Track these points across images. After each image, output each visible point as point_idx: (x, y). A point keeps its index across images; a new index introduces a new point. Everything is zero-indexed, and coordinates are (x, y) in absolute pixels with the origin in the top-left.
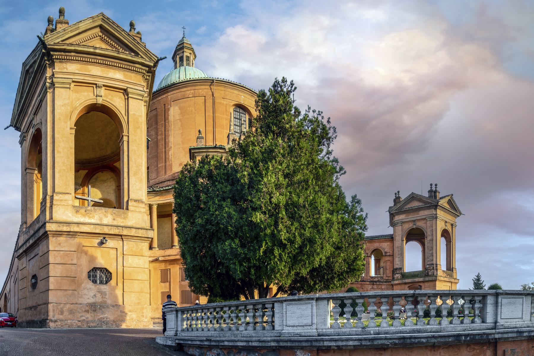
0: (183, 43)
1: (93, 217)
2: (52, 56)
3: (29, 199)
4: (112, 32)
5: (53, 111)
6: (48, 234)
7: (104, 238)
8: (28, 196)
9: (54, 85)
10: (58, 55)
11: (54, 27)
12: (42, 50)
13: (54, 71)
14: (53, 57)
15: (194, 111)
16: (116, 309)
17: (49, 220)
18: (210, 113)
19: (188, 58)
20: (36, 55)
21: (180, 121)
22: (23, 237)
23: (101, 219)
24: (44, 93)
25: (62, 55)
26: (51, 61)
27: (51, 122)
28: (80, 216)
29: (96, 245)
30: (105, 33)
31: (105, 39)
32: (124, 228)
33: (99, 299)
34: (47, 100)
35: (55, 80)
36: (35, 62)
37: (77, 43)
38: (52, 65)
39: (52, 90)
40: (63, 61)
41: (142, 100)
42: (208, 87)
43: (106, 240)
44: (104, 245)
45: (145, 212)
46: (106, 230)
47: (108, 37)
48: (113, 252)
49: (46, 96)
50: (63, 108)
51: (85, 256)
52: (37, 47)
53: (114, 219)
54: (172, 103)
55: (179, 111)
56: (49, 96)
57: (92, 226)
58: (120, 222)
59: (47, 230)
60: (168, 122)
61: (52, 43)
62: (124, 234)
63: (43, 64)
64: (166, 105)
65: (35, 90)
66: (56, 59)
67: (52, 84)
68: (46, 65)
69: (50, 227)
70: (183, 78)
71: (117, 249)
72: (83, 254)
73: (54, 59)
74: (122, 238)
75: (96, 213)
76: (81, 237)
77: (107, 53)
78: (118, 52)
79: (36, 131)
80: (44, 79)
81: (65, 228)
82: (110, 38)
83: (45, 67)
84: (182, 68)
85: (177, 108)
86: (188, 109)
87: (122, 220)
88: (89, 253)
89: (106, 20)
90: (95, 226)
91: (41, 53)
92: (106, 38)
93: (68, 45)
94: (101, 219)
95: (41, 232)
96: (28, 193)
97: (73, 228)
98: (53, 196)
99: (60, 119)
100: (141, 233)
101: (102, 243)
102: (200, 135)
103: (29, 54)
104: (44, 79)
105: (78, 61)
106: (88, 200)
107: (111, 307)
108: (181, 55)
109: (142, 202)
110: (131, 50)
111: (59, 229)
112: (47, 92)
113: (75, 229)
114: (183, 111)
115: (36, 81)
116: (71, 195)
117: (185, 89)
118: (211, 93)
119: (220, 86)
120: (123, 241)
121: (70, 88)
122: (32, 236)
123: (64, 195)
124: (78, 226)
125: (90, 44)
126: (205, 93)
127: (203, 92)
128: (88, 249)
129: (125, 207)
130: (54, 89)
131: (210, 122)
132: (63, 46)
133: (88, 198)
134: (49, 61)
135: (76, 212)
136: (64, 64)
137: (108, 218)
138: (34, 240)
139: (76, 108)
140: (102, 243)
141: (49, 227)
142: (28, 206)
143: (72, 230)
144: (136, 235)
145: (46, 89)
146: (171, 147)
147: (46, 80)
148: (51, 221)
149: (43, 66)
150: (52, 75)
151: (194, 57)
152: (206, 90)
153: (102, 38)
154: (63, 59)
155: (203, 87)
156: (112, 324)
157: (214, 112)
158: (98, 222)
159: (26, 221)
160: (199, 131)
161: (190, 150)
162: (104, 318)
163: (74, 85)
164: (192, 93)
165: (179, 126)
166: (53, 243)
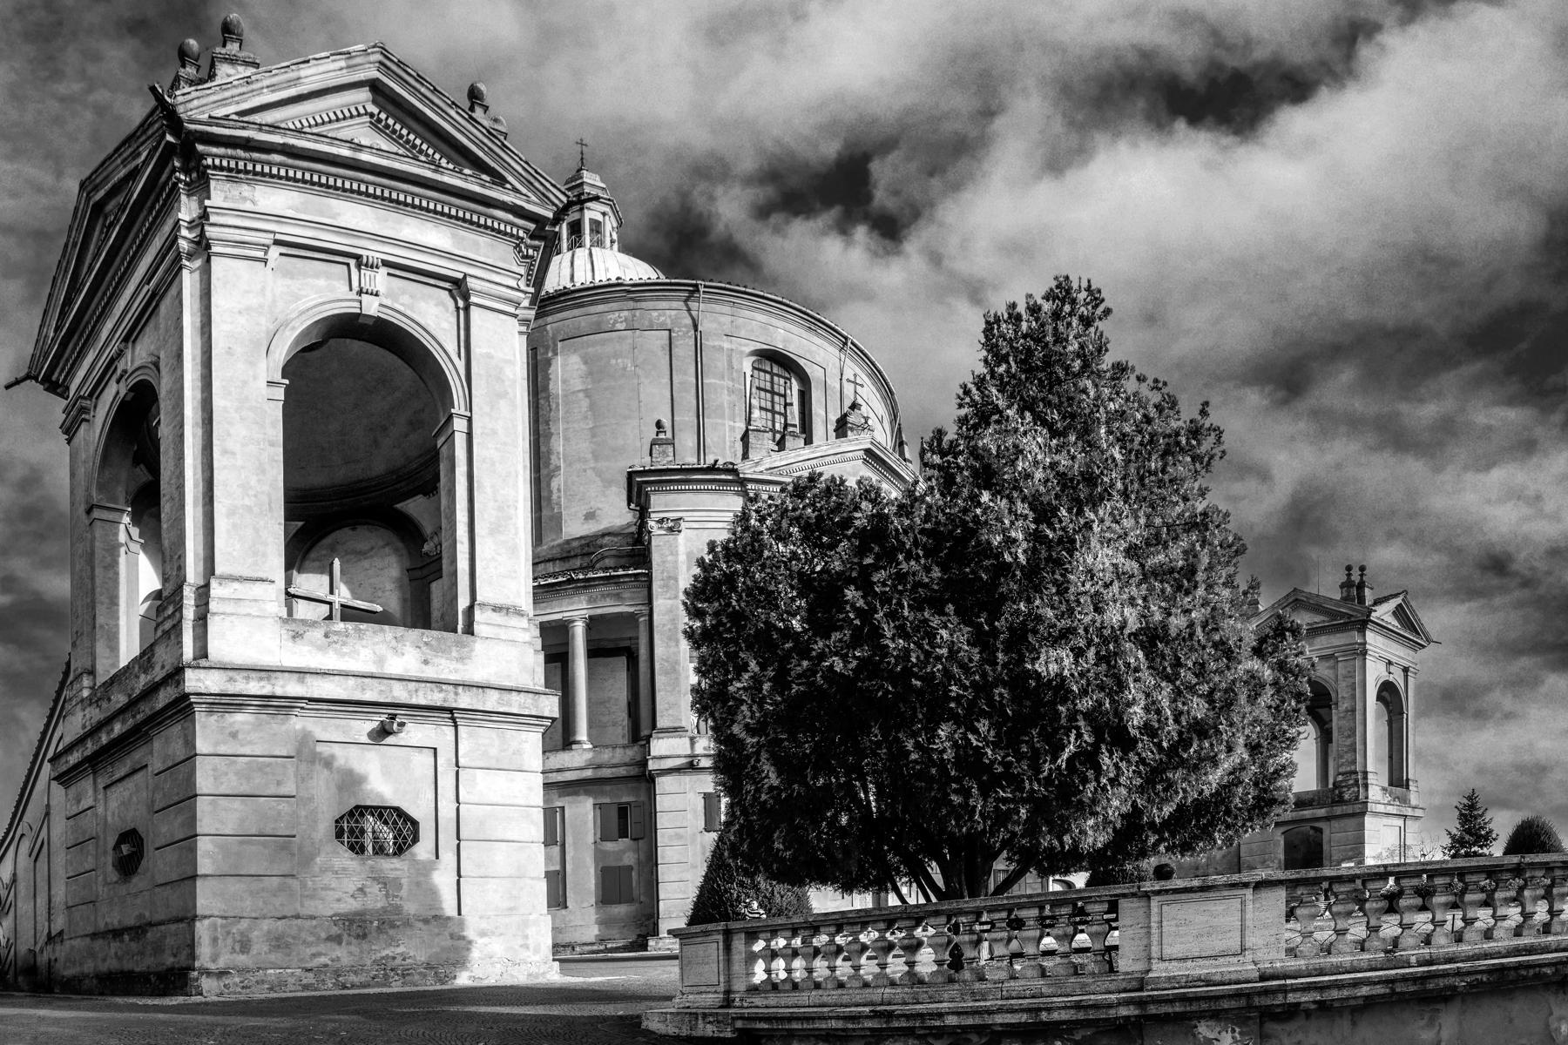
0: (582, 184)
1: (354, 653)
2: (203, 156)
3: (102, 598)
4: (413, 106)
5: (203, 327)
6: (192, 703)
7: (393, 717)
8: (98, 590)
9: (208, 247)
10: (222, 157)
11: (204, 74)
12: (163, 136)
13: (207, 203)
14: (204, 162)
15: (630, 367)
17: (195, 659)
18: (686, 377)
19: (597, 227)
20: (139, 154)
21: (587, 396)
22: (81, 714)
24: (167, 271)
25: (237, 158)
26: (194, 175)
27: (199, 360)
28: (306, 648)
29: (365, 739)
30: (390, 107)
31: (387, 126)
32: (460, 688)
34: (180, 293)
35: (211, 232)
36: (134, 175)
37: (299, 126)
38: (200, 187)
39: (198, 263)
40: (242, 176)
42: (681, 304)
43: (402, 725)
44: (390, 740)
45: (530, 643)
46: (400, 693)
47: (397, 120)
49: (177, 280)
50: (242, 320)
52: (144, 125)
53: (426, 662)
54: (559, 344)
55: (583, 367)
56: (189, 281)
57: (351, 681)
58: (445, 668)
59: (187, 690)
60: (547, 398)
61: (205, 117)
62: (462, 706)
63: (166, 183)
64: (541, 350)
65: (130, 263)
66: (215, 167)
67: (198, 243)
68: (175, 185)
69: (199, 680)
70: (583, 278)
71: (435, 749)
72: (318, 767)
73: (208, 167)
74: (454, 719)
75: (364, 642)
76: (312, 713)
77: (396, 165)
78: (438, 168)
79: (131, 390)
80: (167, 228)
81: (255, 687)
82: (404, 125)
83: (172, 190)
84: (581, 254)
85: (575, 361)
86: (613, 362)
87: (454, 665)
88: (340, 762)
89: (394, 67)
91: (159, 144)
92: (391, 121)
93: (261, 127)
94: (381, 661)
95: (164, 697)
96: (98, 581)
97: (282, 687)
98: (207, 586)
99: (230, 352)
100: (516, 704)
101: (382, 733)
102: (662, 436)
103: (110, 150)
104: (167, 228)
105: (296, 180)
106: (330, 604)
108: (576, 216)
109: (519, 613)
110: (480, 166)
111: (231, 689)
112: (181, 268)
113: (293, 688)
114: (596, 371)
115: (137, 236)
116: (273, 586)
117: (600, 308)
118: (689, 321)
119: (716, 301)
120: (456, 727)
121: (265, 261)
122: (122, 711)
124: (301, 681)
125: (342, 135)
126: (669, 321)
127: (662, 319)
128: (337, 750)
129: (460, 627)
130: (208, 260)
131: (687, 400)
132: (244, 128)
133: (330, 598)
134: (187, 172)
135: (294, 637)
136: (245, 187)
137: (405, 657)
138: (130, 723)
139: (285, 324)
140: (382, 733)
141: (194, 681)
142: (100, 620)
143: (279, 692)
144: (501, 710)
145: (178, 257)
146: (558, 468)
147: (179, 230)
148: (203, 662)
149: (163, 188)
150: (200, 218)
151: (615, 225)
152: (673, 313)
153: (379, 121)
154: (239, 171)
155: (664, 304)
157: (699, 374)
159: (93, 666)
160: (659, 425)
161: (631, 475)
163: (281, 254)
164: (626, 320)
165: (584, 409)
166: (208, 732)
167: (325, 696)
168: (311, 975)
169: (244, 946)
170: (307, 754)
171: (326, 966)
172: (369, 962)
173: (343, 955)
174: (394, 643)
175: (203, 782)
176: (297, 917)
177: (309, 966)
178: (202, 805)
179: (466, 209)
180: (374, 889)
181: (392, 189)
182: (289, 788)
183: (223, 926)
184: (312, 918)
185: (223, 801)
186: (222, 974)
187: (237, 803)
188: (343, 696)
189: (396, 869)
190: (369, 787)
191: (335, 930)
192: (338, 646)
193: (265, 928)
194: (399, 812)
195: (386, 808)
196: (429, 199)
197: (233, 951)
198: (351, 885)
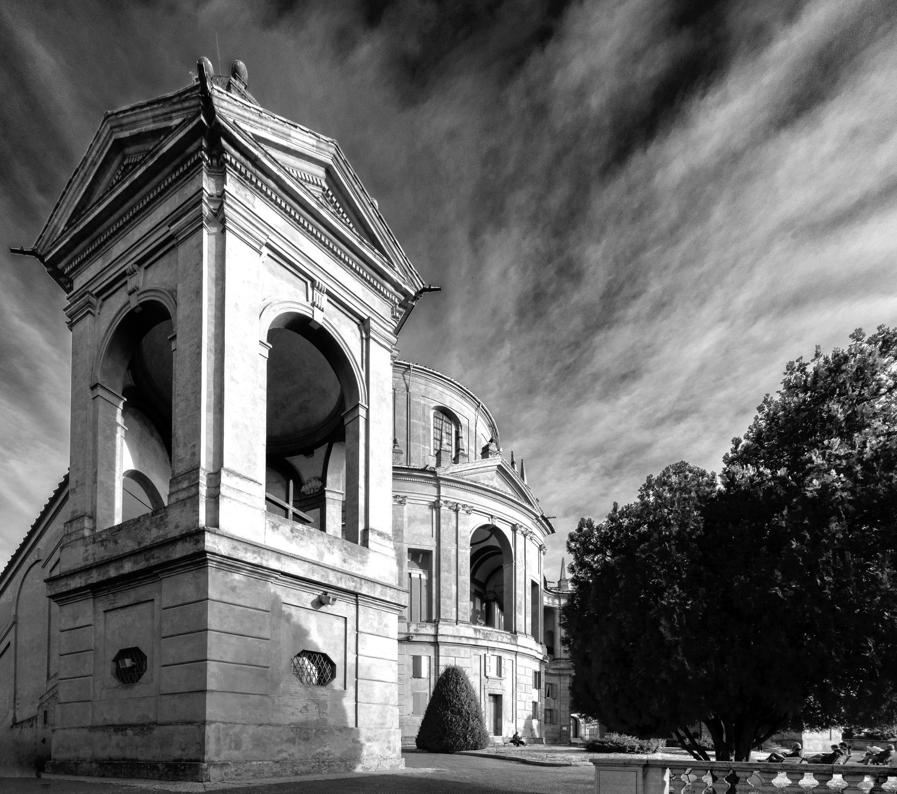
16: (345, 737)
23: (321, 555)
29: (309, 606)
33: (313, 715)
41: (391, 352)
44: (323, 609)
48: (340, 624)
51: (287, 625)
57: (307, 565)
72: (283, 621)
88: (294, 619)
90: (311, 566)
94: (321, 555)
101: (320, 603)
107: (337, 732)
123: (245, 482)
128: (293, 610)
129: (359, 541)
156: (339, 766)
158: (315, 559)
162: (323, 754)
167: (292, 573)
168: (278, 765)
169: (238, 745)
170: (276, 609)
171: (286, 759)
172: (310, 757)
173: (296, 751)
174: (328, 545)
175: (213, 621)
176: (270, 724)
177: (276, 759)
178: (211, 637)
179: (371, 276)
180: (313, 707)
181: (335, 244)
182: (266, 634)
183: (224, 729)
184: (279, 726)
185: (224, 636)
186: (224, 765)
187: (234, 639)
188: (301, 574)
189: (324, 695)
190: (310, 639)
191: (292, 735)
192: (298, 540)
193: (251, 732)
194: (325, 657)
195: (318, 653)
196: (353, 261)
197: (230, 748)
198: (300, 703)
